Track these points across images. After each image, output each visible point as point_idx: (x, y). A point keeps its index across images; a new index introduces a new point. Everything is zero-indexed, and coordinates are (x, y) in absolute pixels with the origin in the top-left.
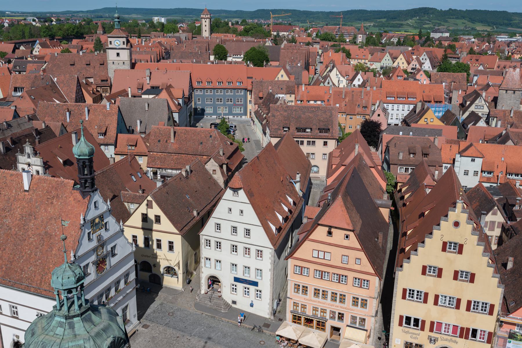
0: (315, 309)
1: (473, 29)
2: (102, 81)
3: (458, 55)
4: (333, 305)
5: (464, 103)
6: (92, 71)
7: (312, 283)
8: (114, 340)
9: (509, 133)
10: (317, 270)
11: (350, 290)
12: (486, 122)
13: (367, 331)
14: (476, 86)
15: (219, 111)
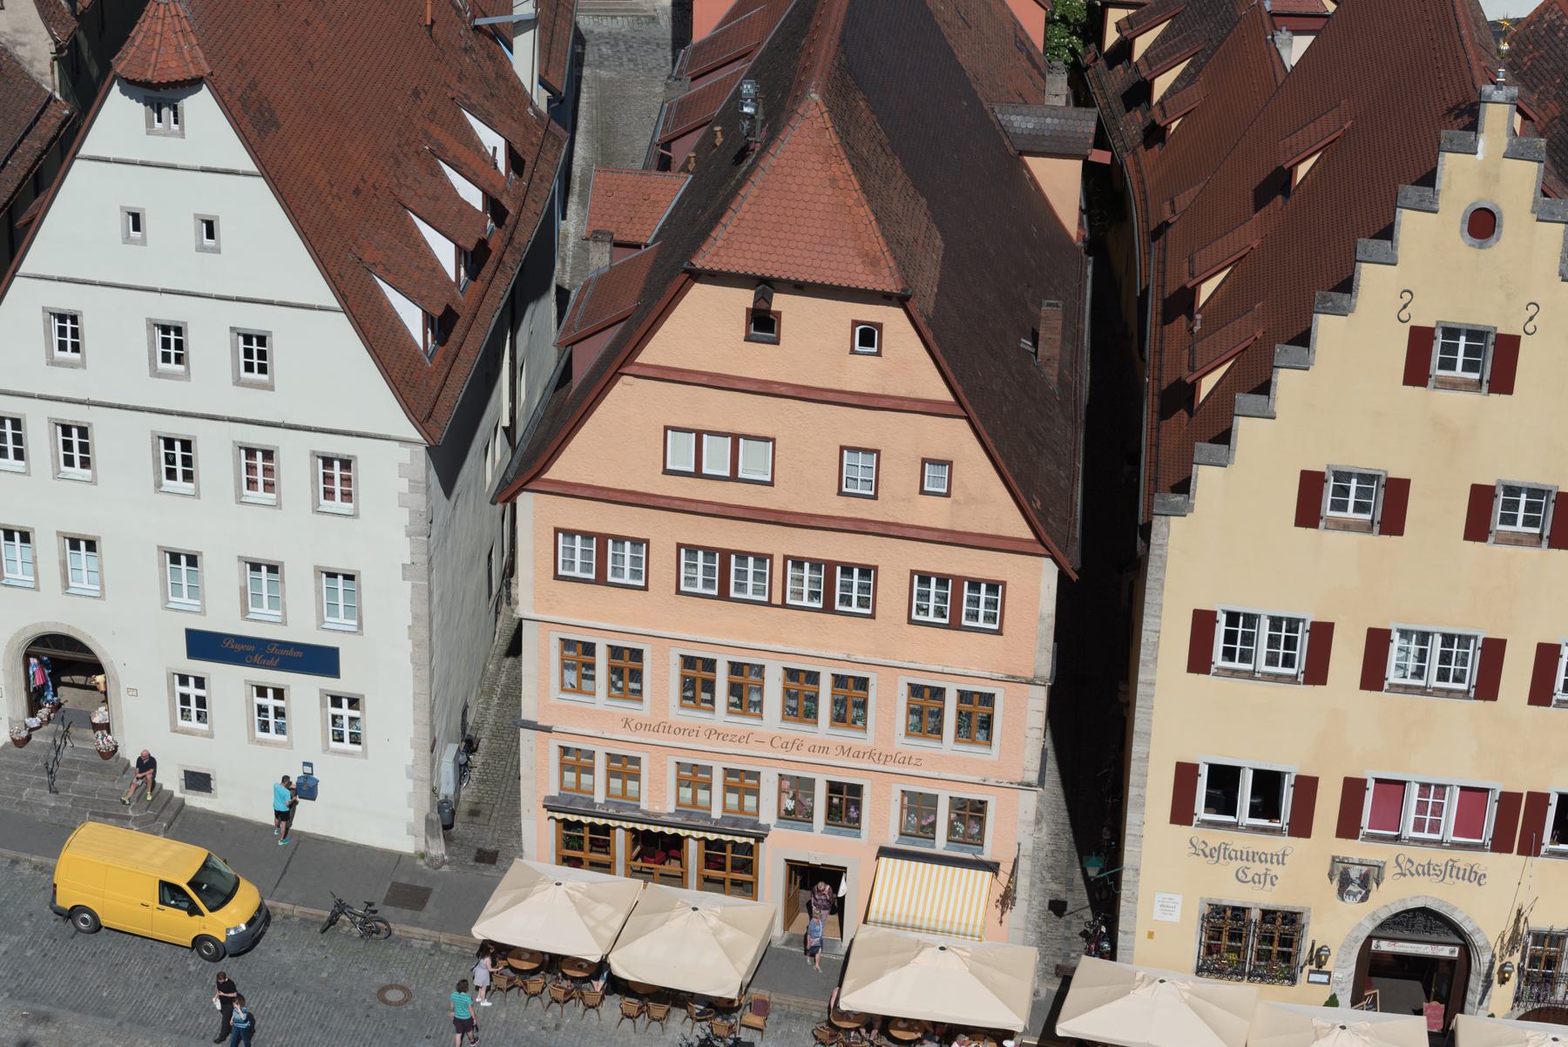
0: (693, 776)
4: (797, 744)
10: (692, 550)
11: (892, 647)
13: (993, 867)
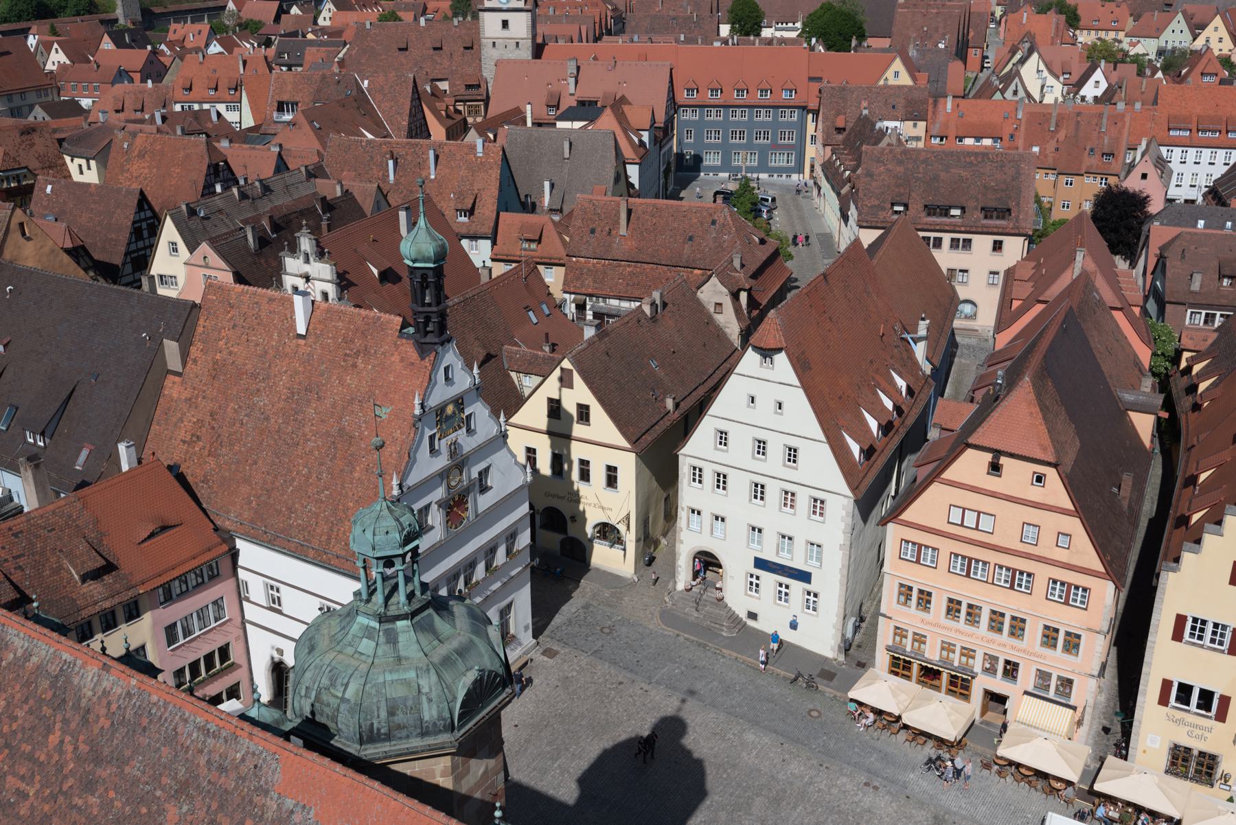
0: (948, 647)
2: (469, 87)
4: (993, 642)
6: (446, 63)
7: (944, 583)
8: (482, 677)
10: (957, 555)
11: (1039, 609)
15: (737, 162)
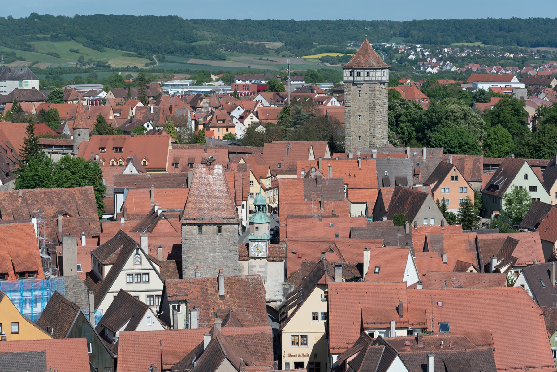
1: (102, 66)
3: (65, 136)
5: (96, 270)
9: (221, 341)
12: (159, 317)
14: (123, 220)
